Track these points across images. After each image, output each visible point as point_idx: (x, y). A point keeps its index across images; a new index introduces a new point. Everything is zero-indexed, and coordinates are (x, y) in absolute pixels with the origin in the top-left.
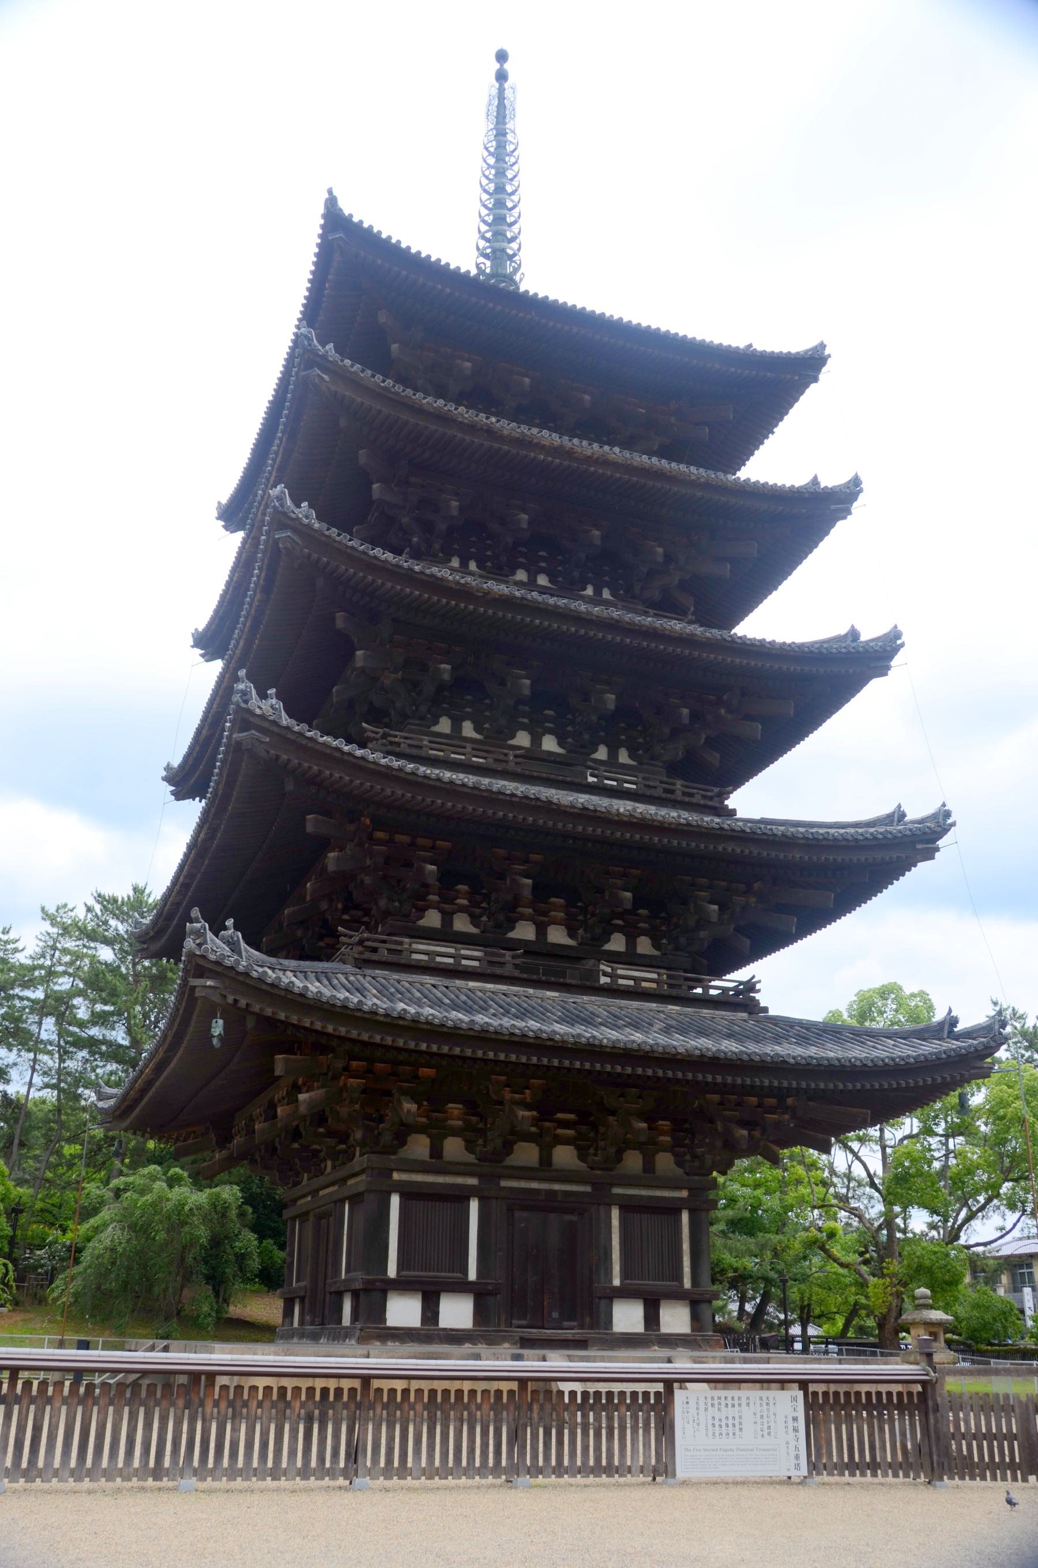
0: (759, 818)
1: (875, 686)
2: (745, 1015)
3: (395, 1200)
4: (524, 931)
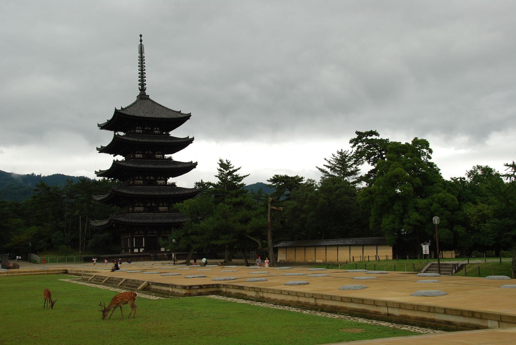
0: (179, 187)
1: (194, 169)
2: (177, 213)
3: (134, 238)
4: (149, 205)
